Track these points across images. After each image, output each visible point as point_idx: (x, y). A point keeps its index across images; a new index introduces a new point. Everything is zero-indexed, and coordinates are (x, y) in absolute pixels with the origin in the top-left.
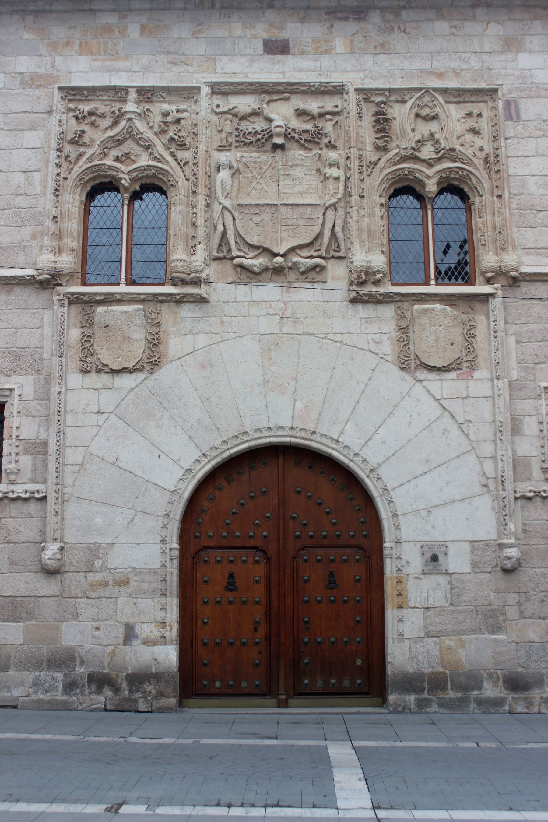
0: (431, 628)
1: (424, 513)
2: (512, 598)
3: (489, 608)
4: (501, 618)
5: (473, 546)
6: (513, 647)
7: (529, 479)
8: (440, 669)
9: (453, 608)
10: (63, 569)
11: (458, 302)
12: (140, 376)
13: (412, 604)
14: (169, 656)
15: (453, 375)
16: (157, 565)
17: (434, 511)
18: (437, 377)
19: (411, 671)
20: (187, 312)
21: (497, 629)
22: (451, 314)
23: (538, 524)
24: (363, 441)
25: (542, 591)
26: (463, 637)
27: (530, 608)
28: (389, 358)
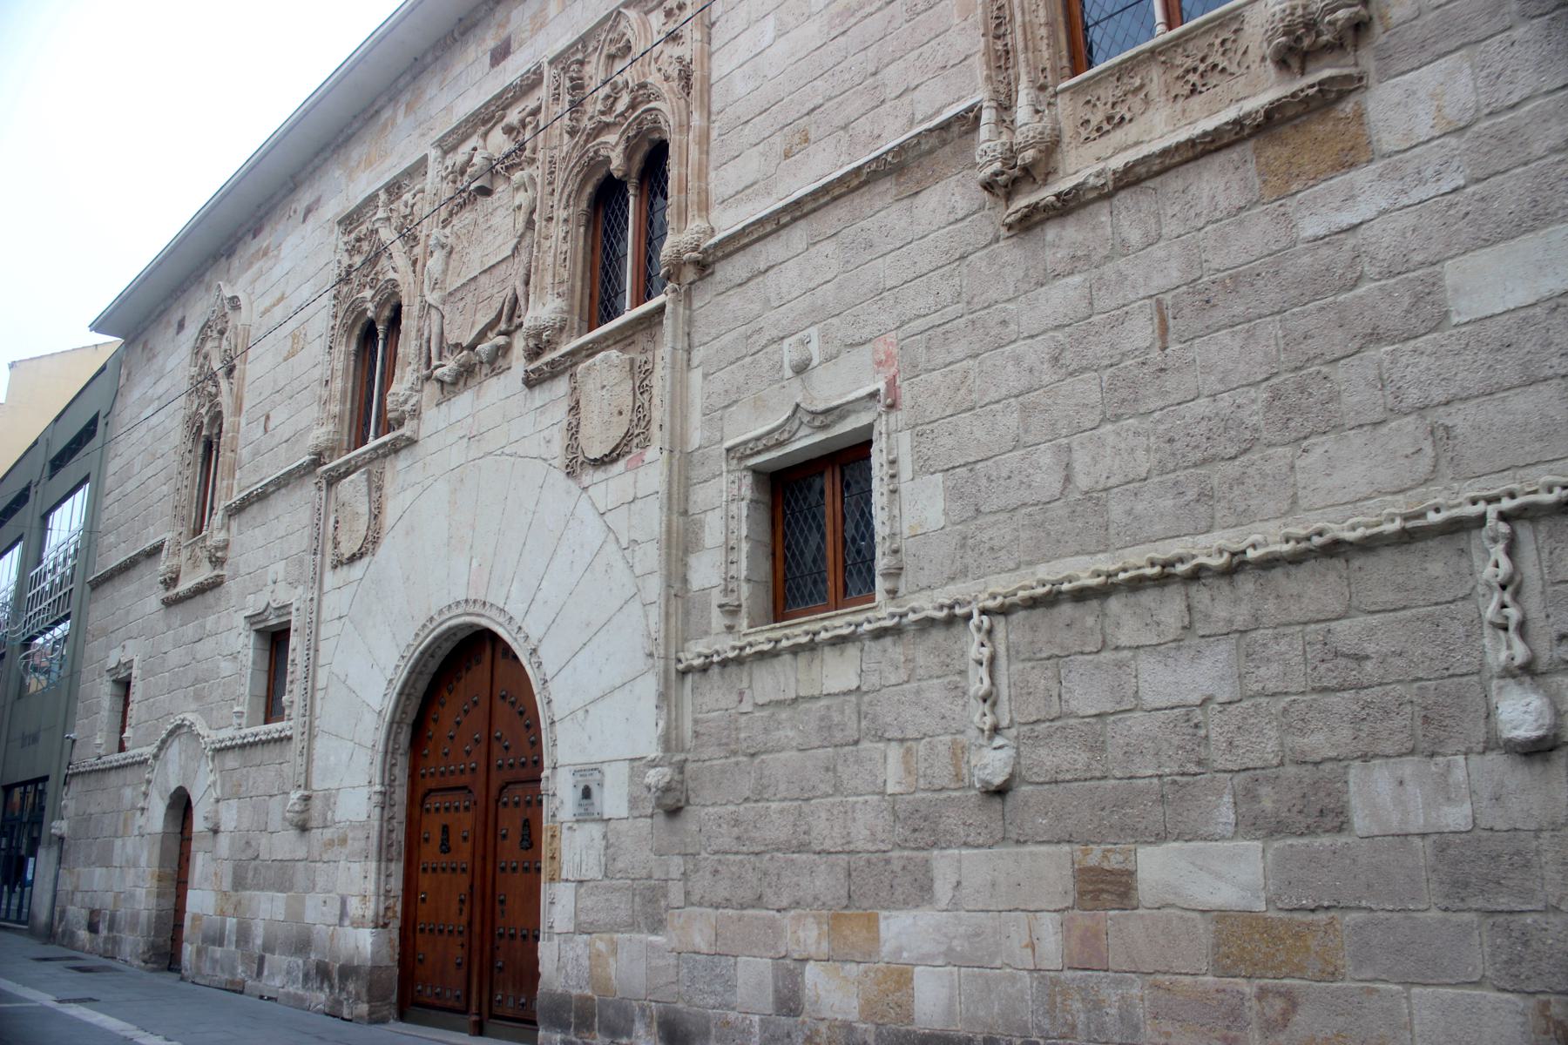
0: (582, 918)
1: (581, 714)
2: (676, 865)
3: (648, 883)
4: (663, 903)
5: (632, 768)
6: (672, 960)
7: (707, 633)
8: (588, 992)
9: (607, 882)
10: (309, 825)
11: (635, 337)
12: (366, 560)
13: (564, 876)
14: (363, 943)
15: (620, 465)
16: (363, 817)
17: (591, 708)
18: (604, 476)
19: (560, 991)
20: (402, 461)
21: (657, 925)
22: (617, 362)
23: (713, 720)
24: (526, 606)
25: (716, 853)
26: (616, 936)
27: (701, 884)
28: (556, 463)
